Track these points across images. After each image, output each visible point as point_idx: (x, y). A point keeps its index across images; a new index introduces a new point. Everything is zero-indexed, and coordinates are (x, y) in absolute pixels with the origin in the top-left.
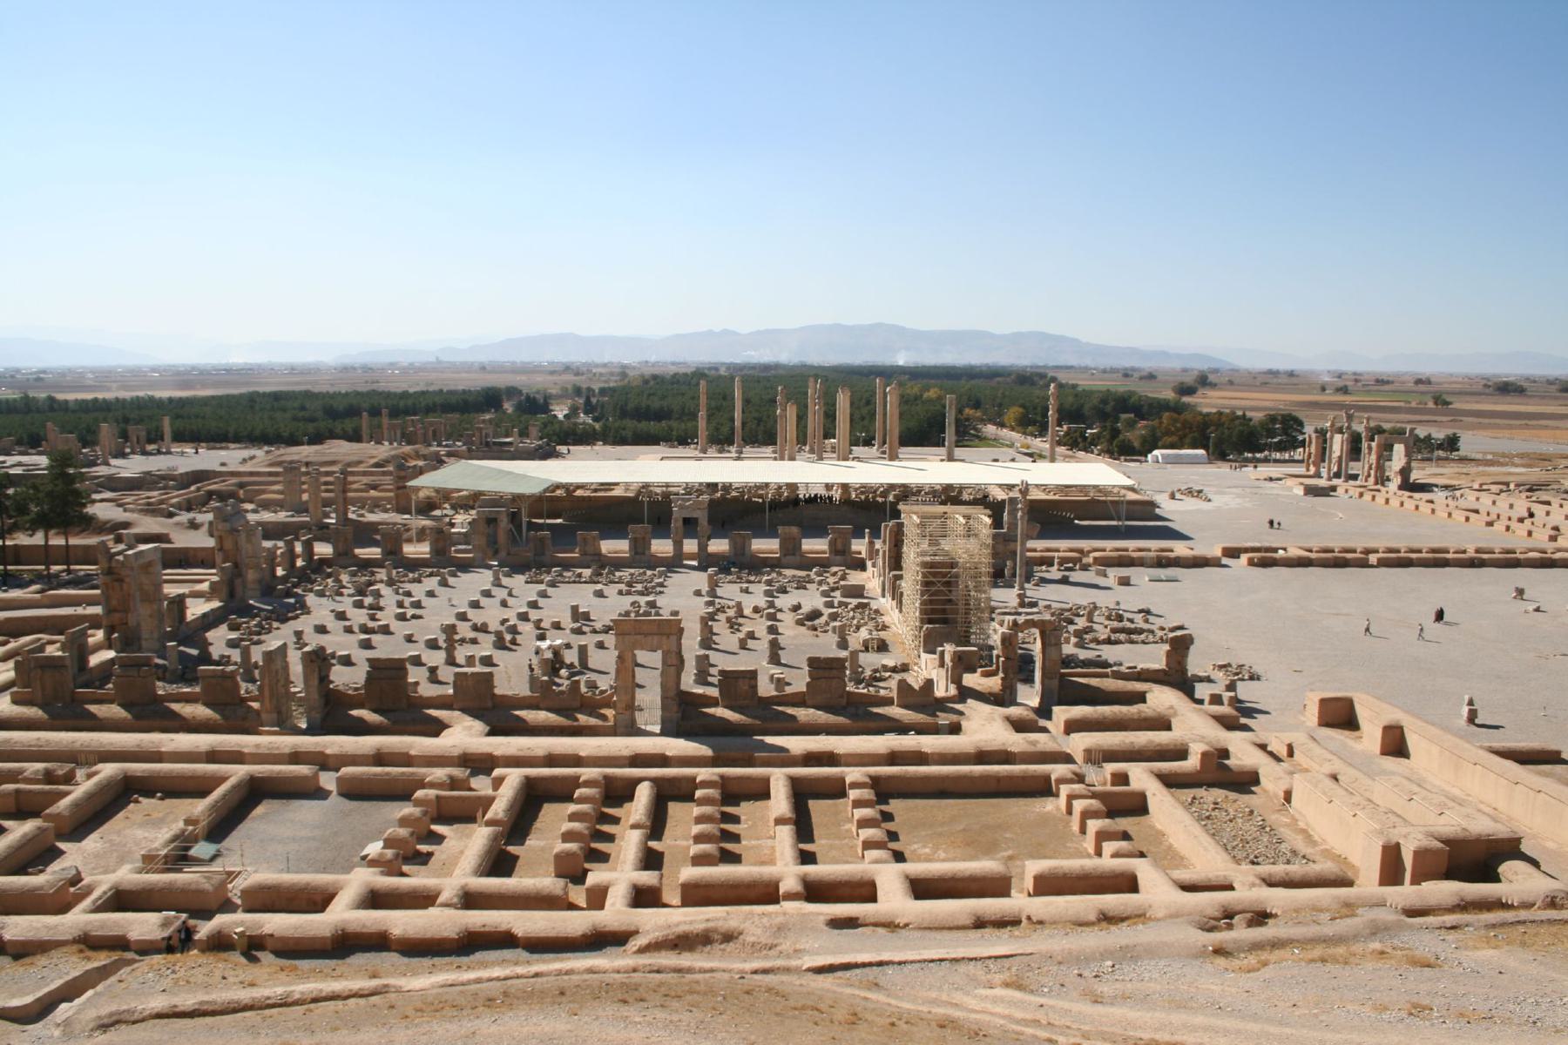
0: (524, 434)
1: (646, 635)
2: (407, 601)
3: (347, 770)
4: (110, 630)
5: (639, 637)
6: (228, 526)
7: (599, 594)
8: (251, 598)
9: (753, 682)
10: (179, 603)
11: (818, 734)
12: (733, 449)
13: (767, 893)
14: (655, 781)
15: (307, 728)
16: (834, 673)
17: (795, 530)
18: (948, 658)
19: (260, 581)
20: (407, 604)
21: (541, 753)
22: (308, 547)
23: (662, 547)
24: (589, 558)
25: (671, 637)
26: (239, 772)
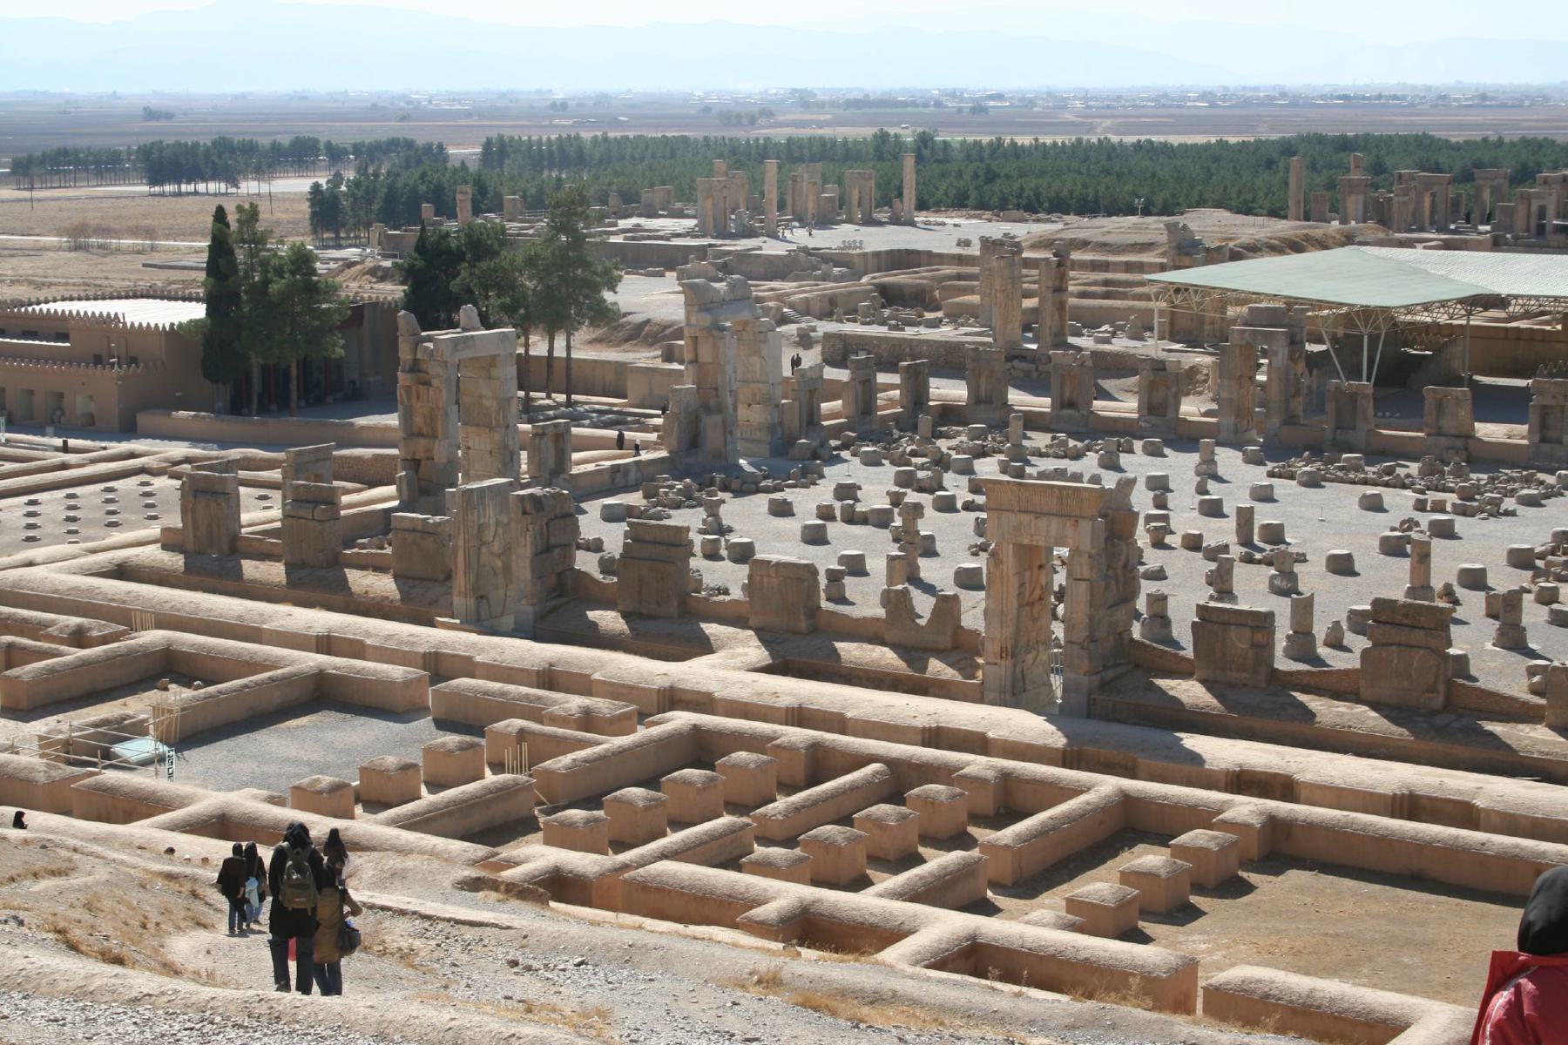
1: (1039, 514)
5: (1025, 518)
6: (706, 319)
8: (744, 456)
9: (1259, 637)
11: (1345, 752)
14: (892, 764)
15: (513, 630)
16: (1418, 636)
19: (771, 429)
21: (784, 702)
24: (1444, 441)
25: (1082, 523)
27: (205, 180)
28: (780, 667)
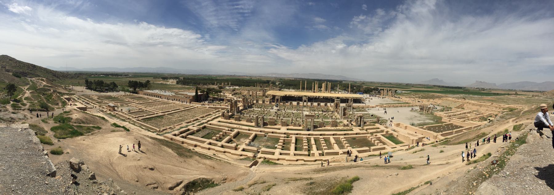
0: (277, 87)
2: (268, 110)
3: (269, 134)
4: (231, 110)
7: (294, 110)
10: (239, 107)
12: (305, 90)
13: (337, 154)
17: (319, 103)
18: (349, 121)
20: (268, 110)
22: (253, 101)
23: (301, 103)
26: (254, 133)
28: (288, 129)
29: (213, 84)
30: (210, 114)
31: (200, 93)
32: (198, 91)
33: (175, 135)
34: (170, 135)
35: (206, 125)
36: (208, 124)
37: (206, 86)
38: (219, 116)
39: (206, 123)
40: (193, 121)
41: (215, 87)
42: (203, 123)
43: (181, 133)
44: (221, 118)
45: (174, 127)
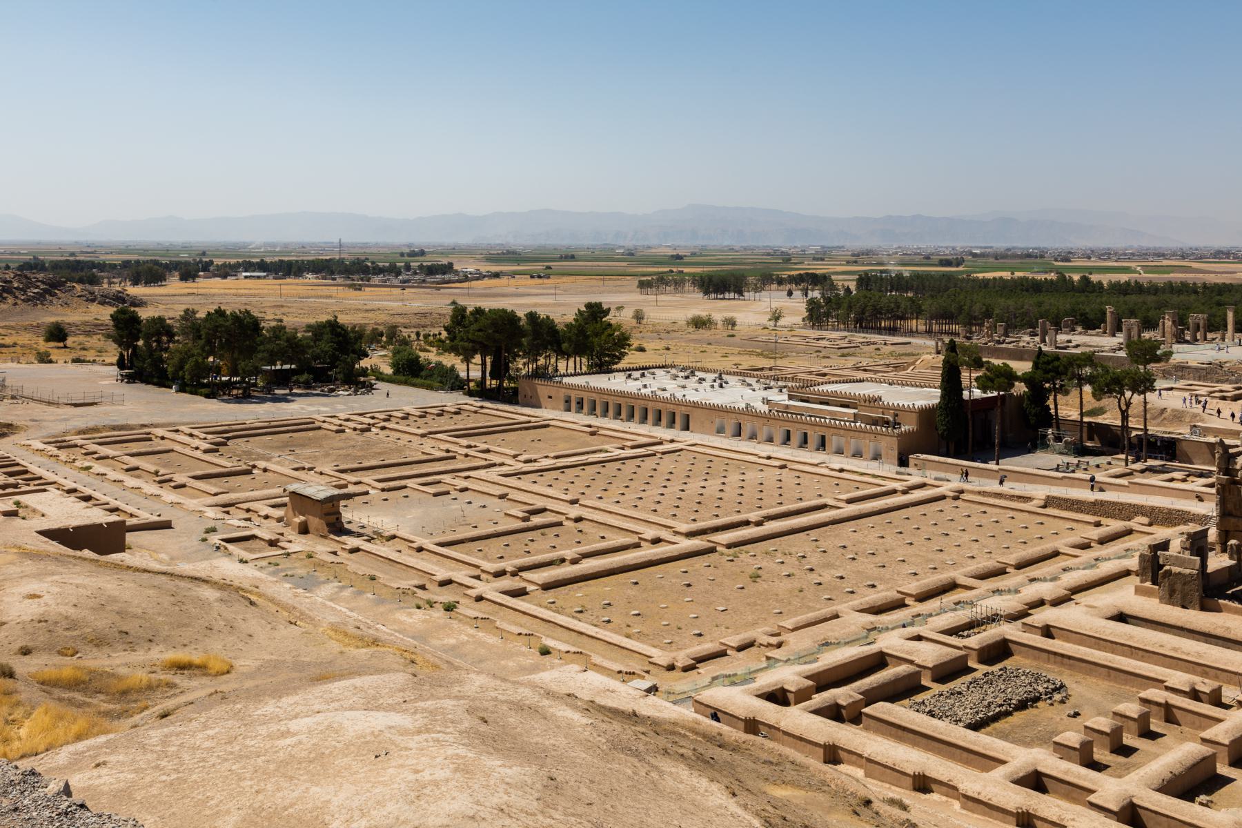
27: (729, 292)
29: (1091, 323)
30: (1056, 554)
31: (978, 393)
32: (965, 375)
33: (778, 697)
34: (741, 700)
35: (1010, 631)
36: (1029, 628)
37: (1033, 334)
38: (1127, 573)
39: (1013, 618)
40: (923, 597)
41: (1106, 343)
42: (993, 619)
43: (824, 681)
44: (1139, 591)
45: (774, 640)
